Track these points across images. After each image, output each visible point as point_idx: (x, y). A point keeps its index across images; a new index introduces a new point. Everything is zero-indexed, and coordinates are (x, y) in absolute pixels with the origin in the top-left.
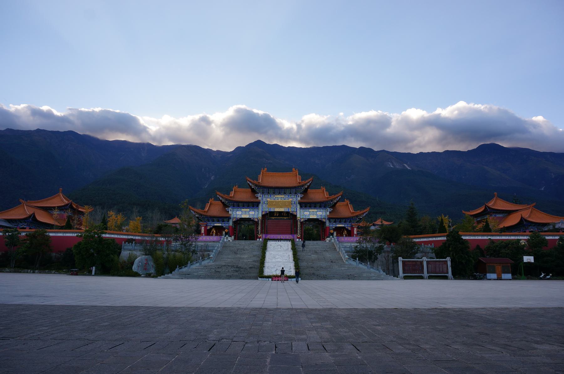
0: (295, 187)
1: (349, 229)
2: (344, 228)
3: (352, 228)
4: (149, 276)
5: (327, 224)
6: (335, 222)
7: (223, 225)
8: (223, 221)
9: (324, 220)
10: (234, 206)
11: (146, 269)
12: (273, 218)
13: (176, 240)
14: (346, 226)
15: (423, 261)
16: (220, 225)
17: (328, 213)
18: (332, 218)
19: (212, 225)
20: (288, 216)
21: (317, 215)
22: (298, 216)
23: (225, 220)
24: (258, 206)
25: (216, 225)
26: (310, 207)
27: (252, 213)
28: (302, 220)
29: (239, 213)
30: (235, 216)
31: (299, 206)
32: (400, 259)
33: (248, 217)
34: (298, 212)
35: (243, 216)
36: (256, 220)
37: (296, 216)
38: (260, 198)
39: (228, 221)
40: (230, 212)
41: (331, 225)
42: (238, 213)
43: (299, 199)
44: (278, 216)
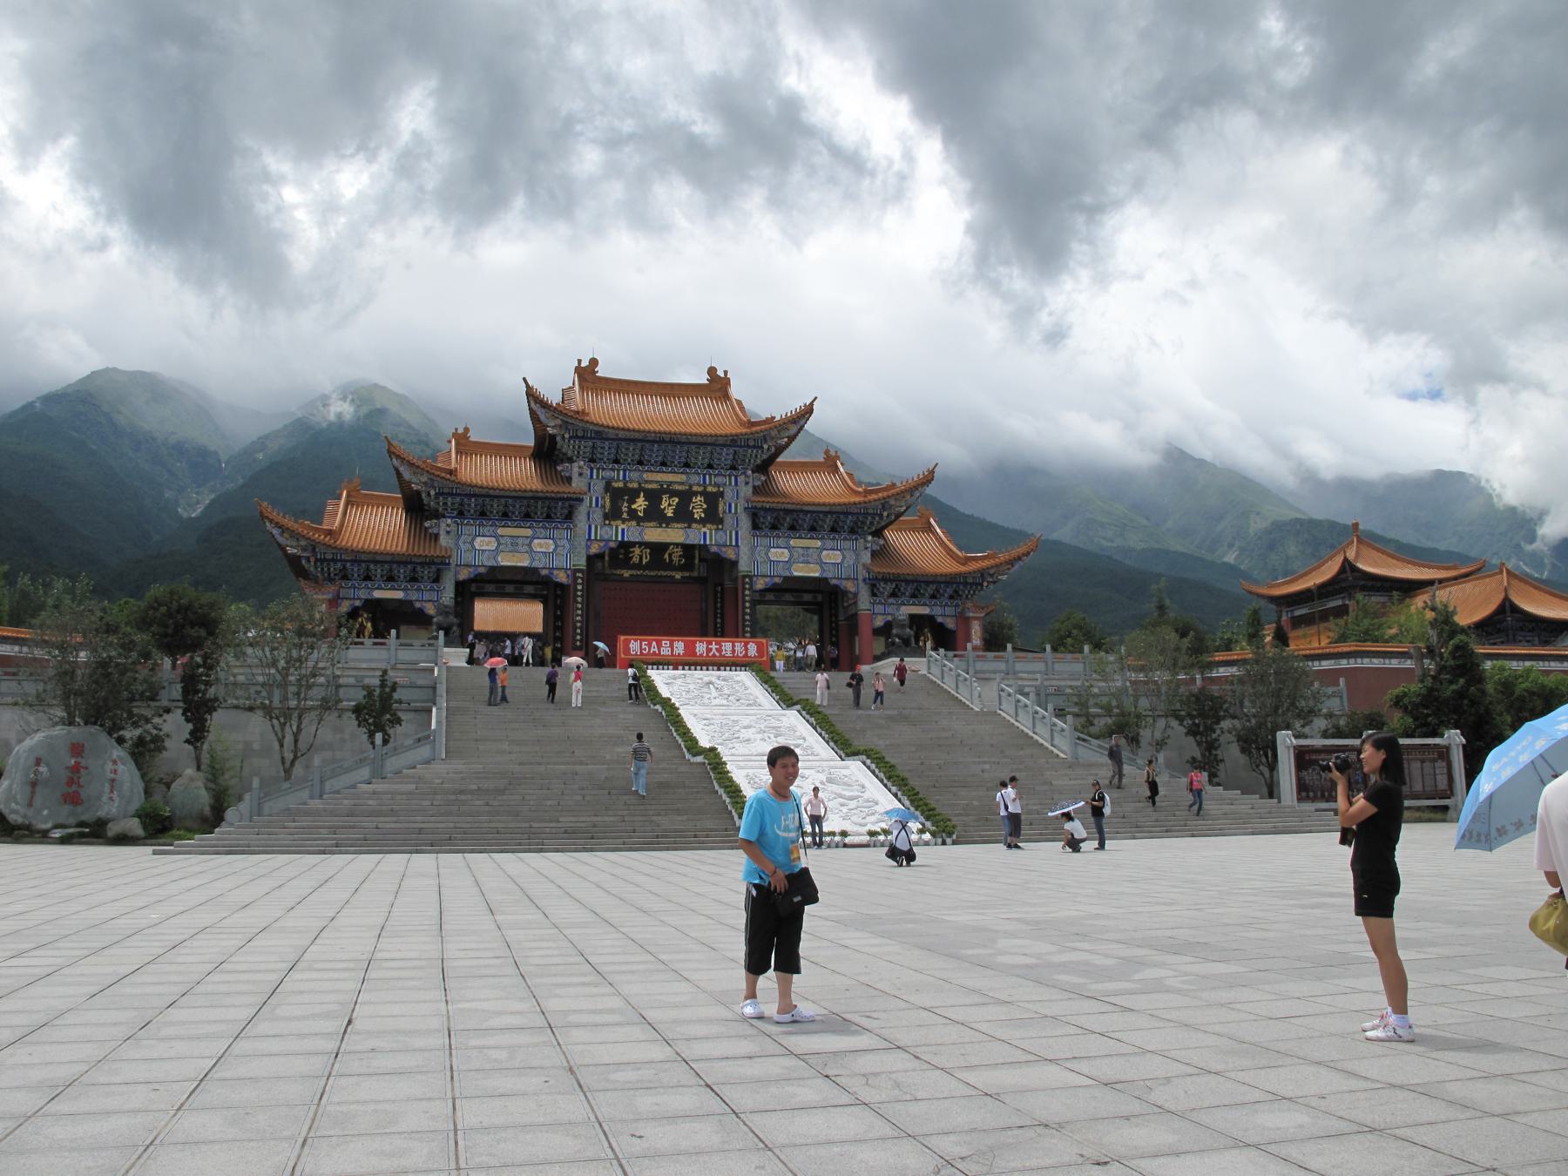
0: (733, 441)
1: (950, 624)
2: (930, 619)
3: (965, 621)
4: (95, 832)
5: (864, 602)
6: (893, 595)
7: (413, 596)
8: (414, 579)
9: (850, 586)
10: (461, 514)
11: (73, 799)
12: (626, 574)
13: (247, 630)
14: (937, 611)
15: (1448, 748)
16: (399, 595)
17: (866, 557)
18: (886, 579)
19: (363, 594)
20: (688, 566)
21: (821, 563)
22: (743, 566)
23: (426, 572)
24: (569, 516)
25: (378, 594)
26: (792, 528)
27: (543, 545)
28: (760, 584)
29: (484, 543)
30: (467, 558)
31: (745, 523)
32: (1286, 740)
33: (526, 564)
34: (744, 550)
35: (505, 561)
36: (562, 577)
37: (735, 564)
38: (578, 484)
39: (437, 580)
40: (444, 540)
41: (879, 609)
42: (480, 543)
43: (747, 491)
44: (648, 567)
